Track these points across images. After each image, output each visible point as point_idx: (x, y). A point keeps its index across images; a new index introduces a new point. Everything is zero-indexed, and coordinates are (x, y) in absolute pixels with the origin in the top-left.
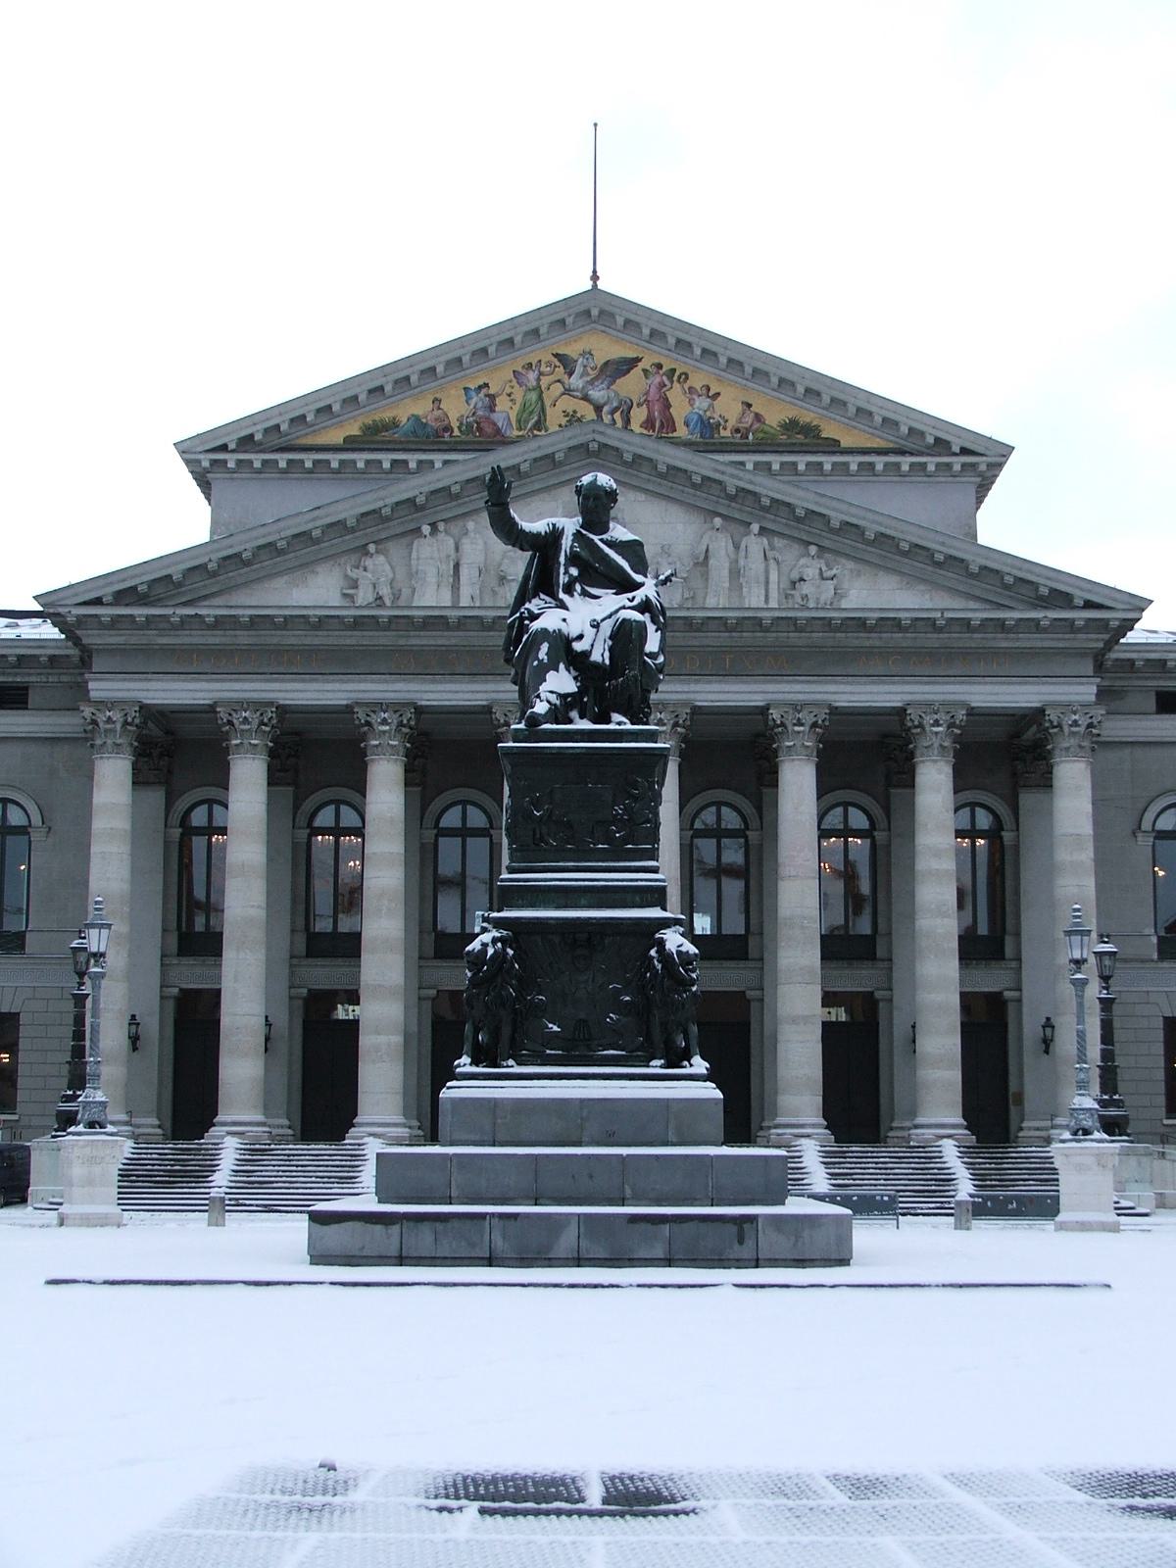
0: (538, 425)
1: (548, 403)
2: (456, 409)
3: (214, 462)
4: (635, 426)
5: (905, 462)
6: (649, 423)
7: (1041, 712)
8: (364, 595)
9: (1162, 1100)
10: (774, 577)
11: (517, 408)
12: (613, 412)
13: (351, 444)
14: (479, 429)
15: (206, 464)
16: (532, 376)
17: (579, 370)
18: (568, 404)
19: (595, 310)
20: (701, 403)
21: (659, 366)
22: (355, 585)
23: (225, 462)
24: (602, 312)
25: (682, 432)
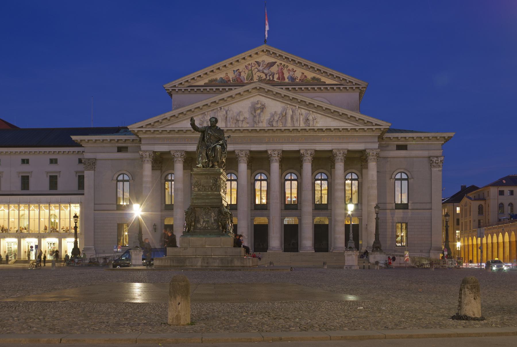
0: (252, 79)
1: (254, 73)
2: (231, 76)
3: (173, 90)
4: (275, 79)
5: (342, 87)
6: (279, 78)
7: (365, 150)
10: (301, 119)
11: (246, 75)
12: (270, 76)
13: (206, 85)
14: (237, 80)
15: (171, 90)
16: (250, 67)
17: (261, 65)
18: (259, 74)
20: (292, 73)
21: (281, 64)
23: (175, 90)
24: (267, 50)
25: (287, 80)
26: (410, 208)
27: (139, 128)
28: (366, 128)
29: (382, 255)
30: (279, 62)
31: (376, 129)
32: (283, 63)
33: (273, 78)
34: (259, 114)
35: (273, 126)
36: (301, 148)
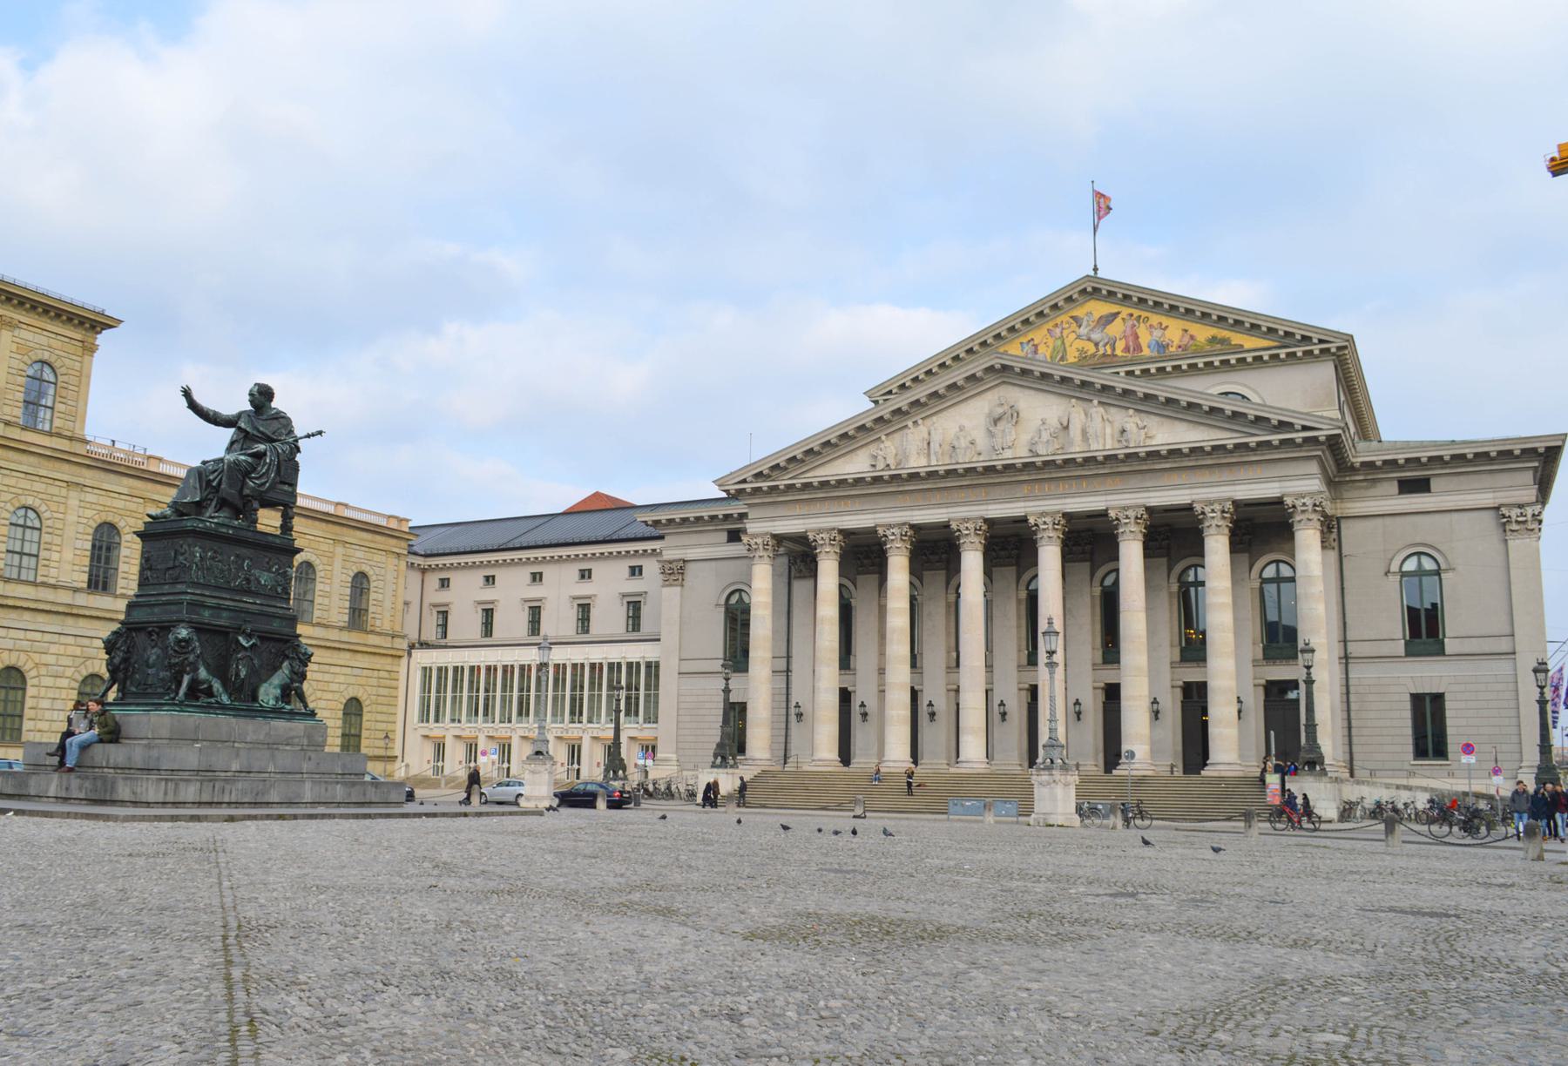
4: (1119, 352)
6: (1127, 349)
8: (881, 465)
9: (1410, 748)
10: (1108, 431)
16: (1058, 331)
18: (1079, 344)
19: (1093, 289)
20: (1157, 333)
22: (875, 457)
25: (1146, 352)
26: (1448, 650)
28: (1275, 438)
29: (1322, 785)
30: (1125, 311)
31: (1306, 440)
32: (1136, 313)
33: (1114, 349)
36: (1109, 504)
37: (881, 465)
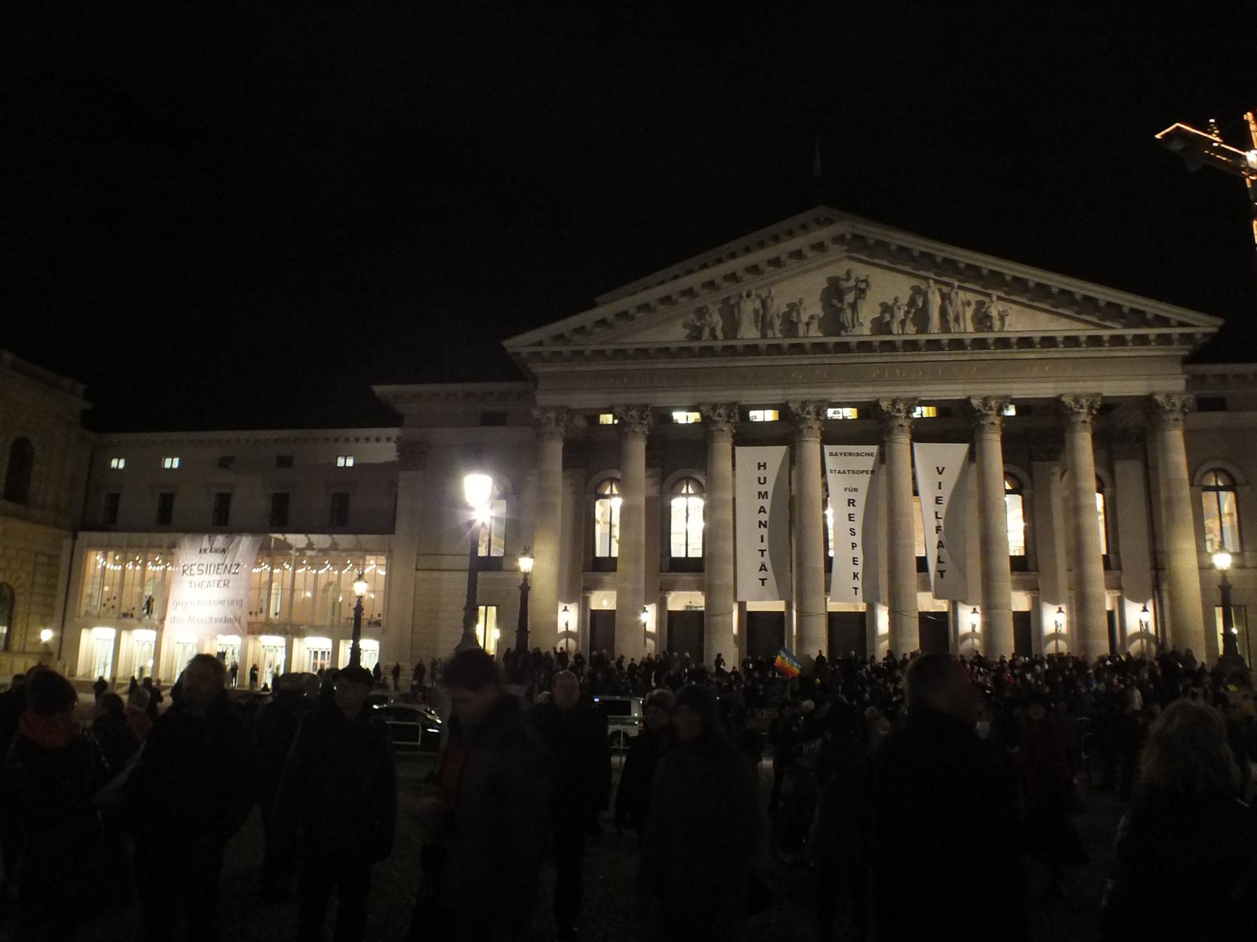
27: (534, 345)
34: (854, 306)
35: (890, 333)
37: (706, 333)
